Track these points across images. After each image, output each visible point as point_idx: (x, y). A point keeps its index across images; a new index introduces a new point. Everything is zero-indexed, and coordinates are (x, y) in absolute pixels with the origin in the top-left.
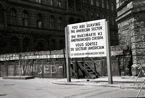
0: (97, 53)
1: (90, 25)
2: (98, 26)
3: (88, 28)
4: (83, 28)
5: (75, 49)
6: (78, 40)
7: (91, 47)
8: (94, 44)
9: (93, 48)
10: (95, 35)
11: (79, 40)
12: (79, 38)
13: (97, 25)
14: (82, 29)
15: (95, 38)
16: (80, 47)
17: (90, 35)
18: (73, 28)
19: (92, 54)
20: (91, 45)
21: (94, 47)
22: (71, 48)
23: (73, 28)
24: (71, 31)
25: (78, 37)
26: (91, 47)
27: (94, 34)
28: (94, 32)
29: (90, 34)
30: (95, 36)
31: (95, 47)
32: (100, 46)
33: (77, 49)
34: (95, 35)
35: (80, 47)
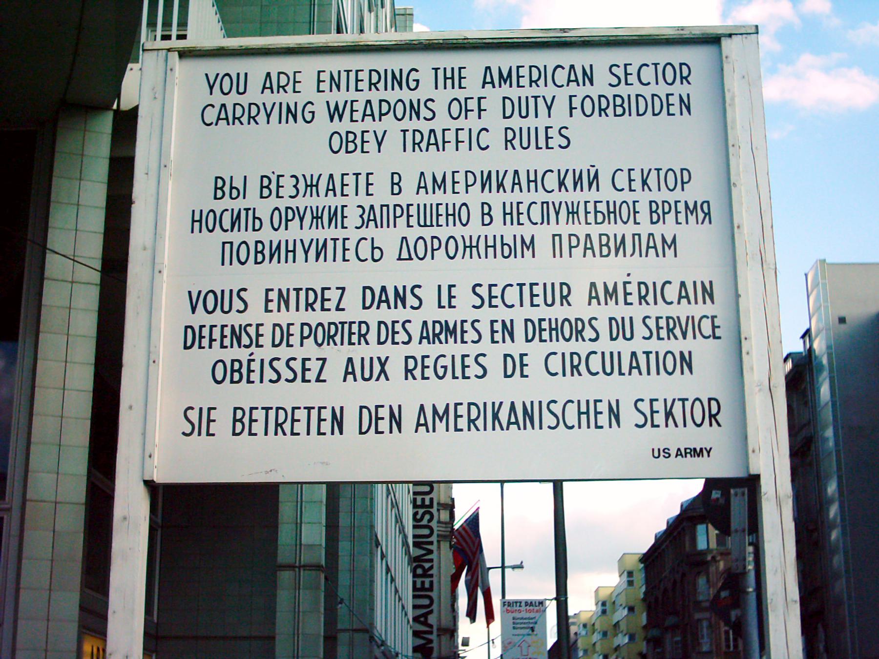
0: (615, 414)
19: (526, 416)
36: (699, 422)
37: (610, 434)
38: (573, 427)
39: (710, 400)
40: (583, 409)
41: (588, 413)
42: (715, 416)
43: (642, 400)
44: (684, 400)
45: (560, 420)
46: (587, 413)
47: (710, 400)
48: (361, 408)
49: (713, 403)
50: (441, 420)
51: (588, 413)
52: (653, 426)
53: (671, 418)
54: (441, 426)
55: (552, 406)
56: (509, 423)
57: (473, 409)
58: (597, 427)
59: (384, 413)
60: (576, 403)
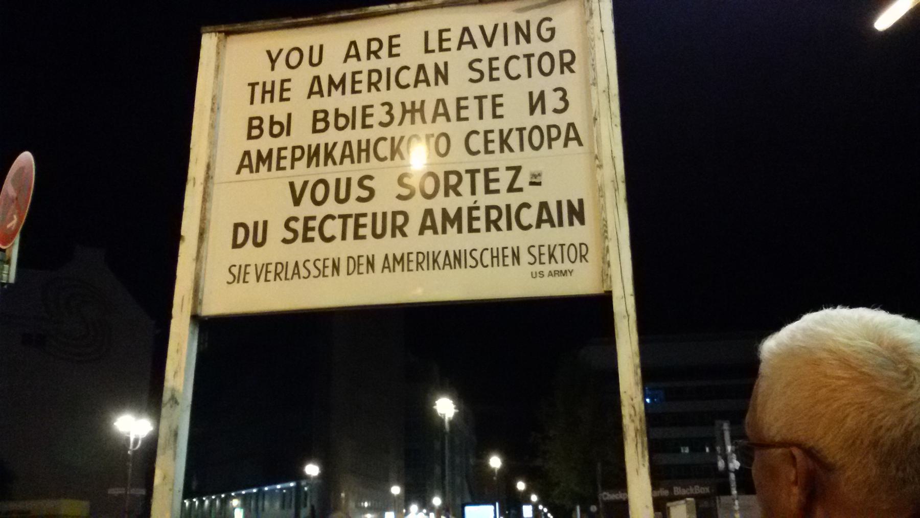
0: (516, 257)
1: (454, 36)
2: (536, 47)
3: (429, 62)
4: (383, 63)
5: (277, 232)
6: (313, 155)
7: (452, 214)
8: (488, 181)
9: (471, 219)
10: (495, 116)
11: (329, 155)
12: (332, 136)
13: (523, 34)
14: (365, 65)
15: (495, 136)
16: (331, 207)
17: (446, 114)
18: (273, 61)
19: (457, 260)
20: (455, 188)
21: (481, 214)
22: (236, 226)
23: (273, 61)
24: (253, 85)
25: (321, 125)
26: (452, 214)
27: (487, 104)
28: (487, 88)
29: (441, 102)
30: (496, 125)
31: (494, 214)
32: (544, 206)
33: (303, 231)
34: (495, 116)
35: (331, 207)
36: (573, 259)
37: (513, 269)
38: (487, 266)
39: (581, 244)
40: (495, 254)
41: (498, 257)
42: (584, 256)
43: (533, 246)
44: (562, 245)
45: (479, 262)
46: (497, 257)
47: (581, 244)
48: (349, 258)
49: (583, 247)
50: (399, 263)
51: (498, 257)
52: (541, 263)
53: (553, 260)
54: (398, 268)
55: (474, 252)
56: (445, 264)
57: (421, 256)
58: (504, 265)
59: (363, 261)
60: (489, 251)
